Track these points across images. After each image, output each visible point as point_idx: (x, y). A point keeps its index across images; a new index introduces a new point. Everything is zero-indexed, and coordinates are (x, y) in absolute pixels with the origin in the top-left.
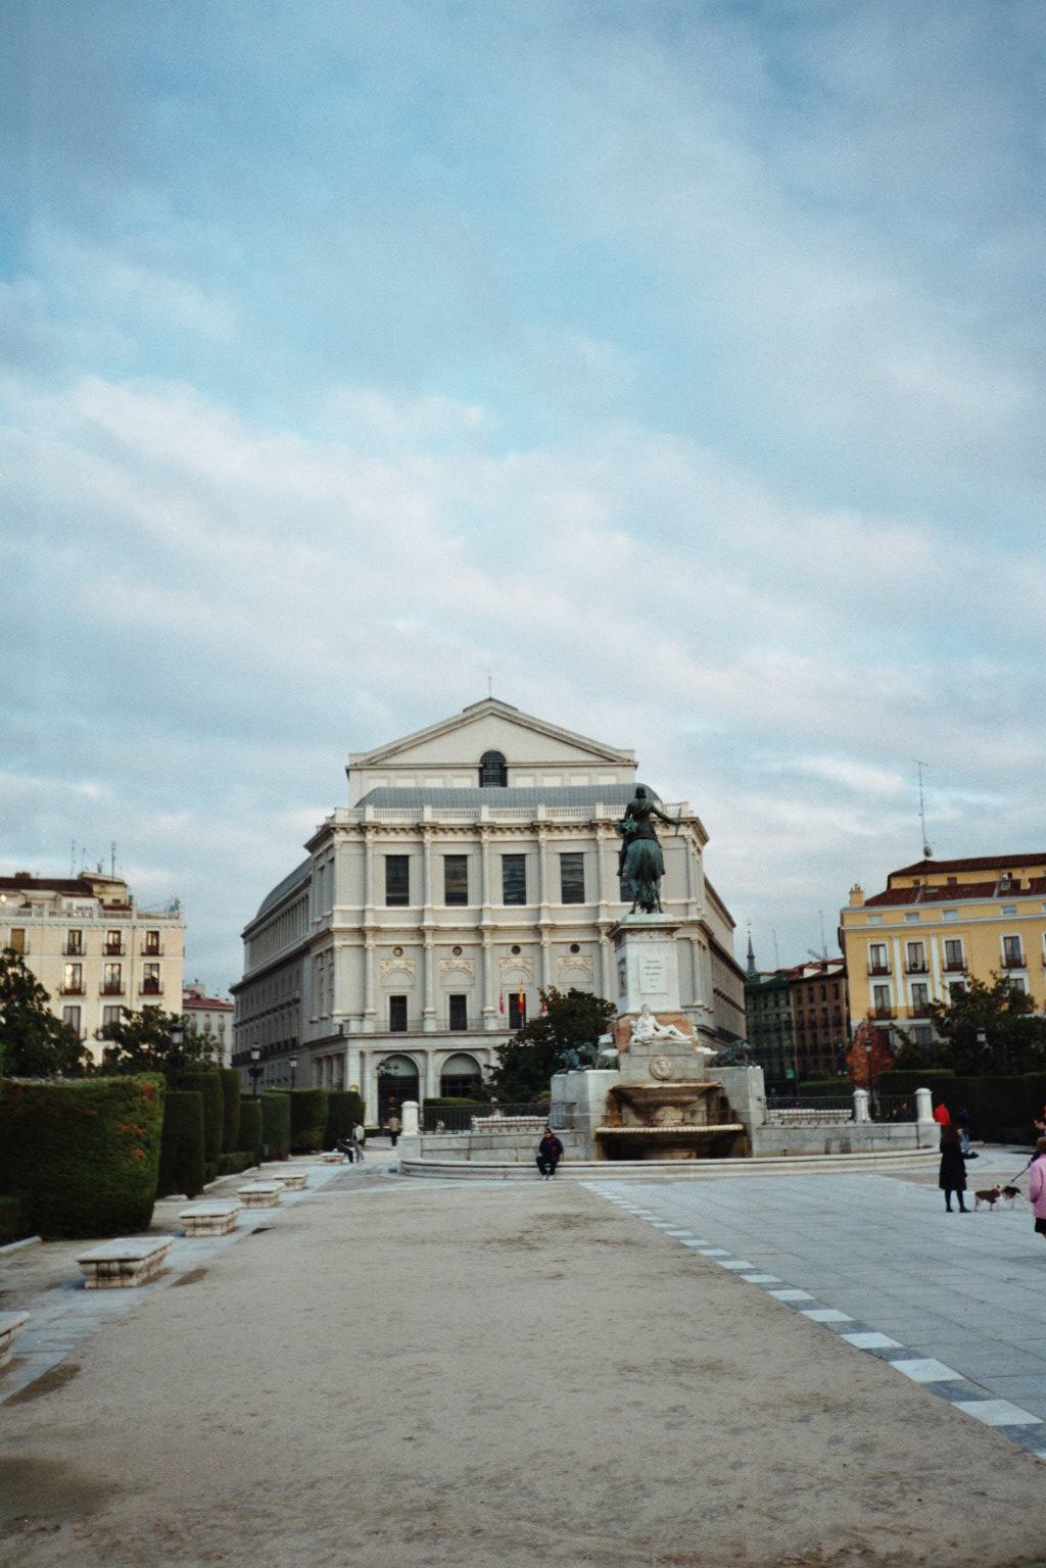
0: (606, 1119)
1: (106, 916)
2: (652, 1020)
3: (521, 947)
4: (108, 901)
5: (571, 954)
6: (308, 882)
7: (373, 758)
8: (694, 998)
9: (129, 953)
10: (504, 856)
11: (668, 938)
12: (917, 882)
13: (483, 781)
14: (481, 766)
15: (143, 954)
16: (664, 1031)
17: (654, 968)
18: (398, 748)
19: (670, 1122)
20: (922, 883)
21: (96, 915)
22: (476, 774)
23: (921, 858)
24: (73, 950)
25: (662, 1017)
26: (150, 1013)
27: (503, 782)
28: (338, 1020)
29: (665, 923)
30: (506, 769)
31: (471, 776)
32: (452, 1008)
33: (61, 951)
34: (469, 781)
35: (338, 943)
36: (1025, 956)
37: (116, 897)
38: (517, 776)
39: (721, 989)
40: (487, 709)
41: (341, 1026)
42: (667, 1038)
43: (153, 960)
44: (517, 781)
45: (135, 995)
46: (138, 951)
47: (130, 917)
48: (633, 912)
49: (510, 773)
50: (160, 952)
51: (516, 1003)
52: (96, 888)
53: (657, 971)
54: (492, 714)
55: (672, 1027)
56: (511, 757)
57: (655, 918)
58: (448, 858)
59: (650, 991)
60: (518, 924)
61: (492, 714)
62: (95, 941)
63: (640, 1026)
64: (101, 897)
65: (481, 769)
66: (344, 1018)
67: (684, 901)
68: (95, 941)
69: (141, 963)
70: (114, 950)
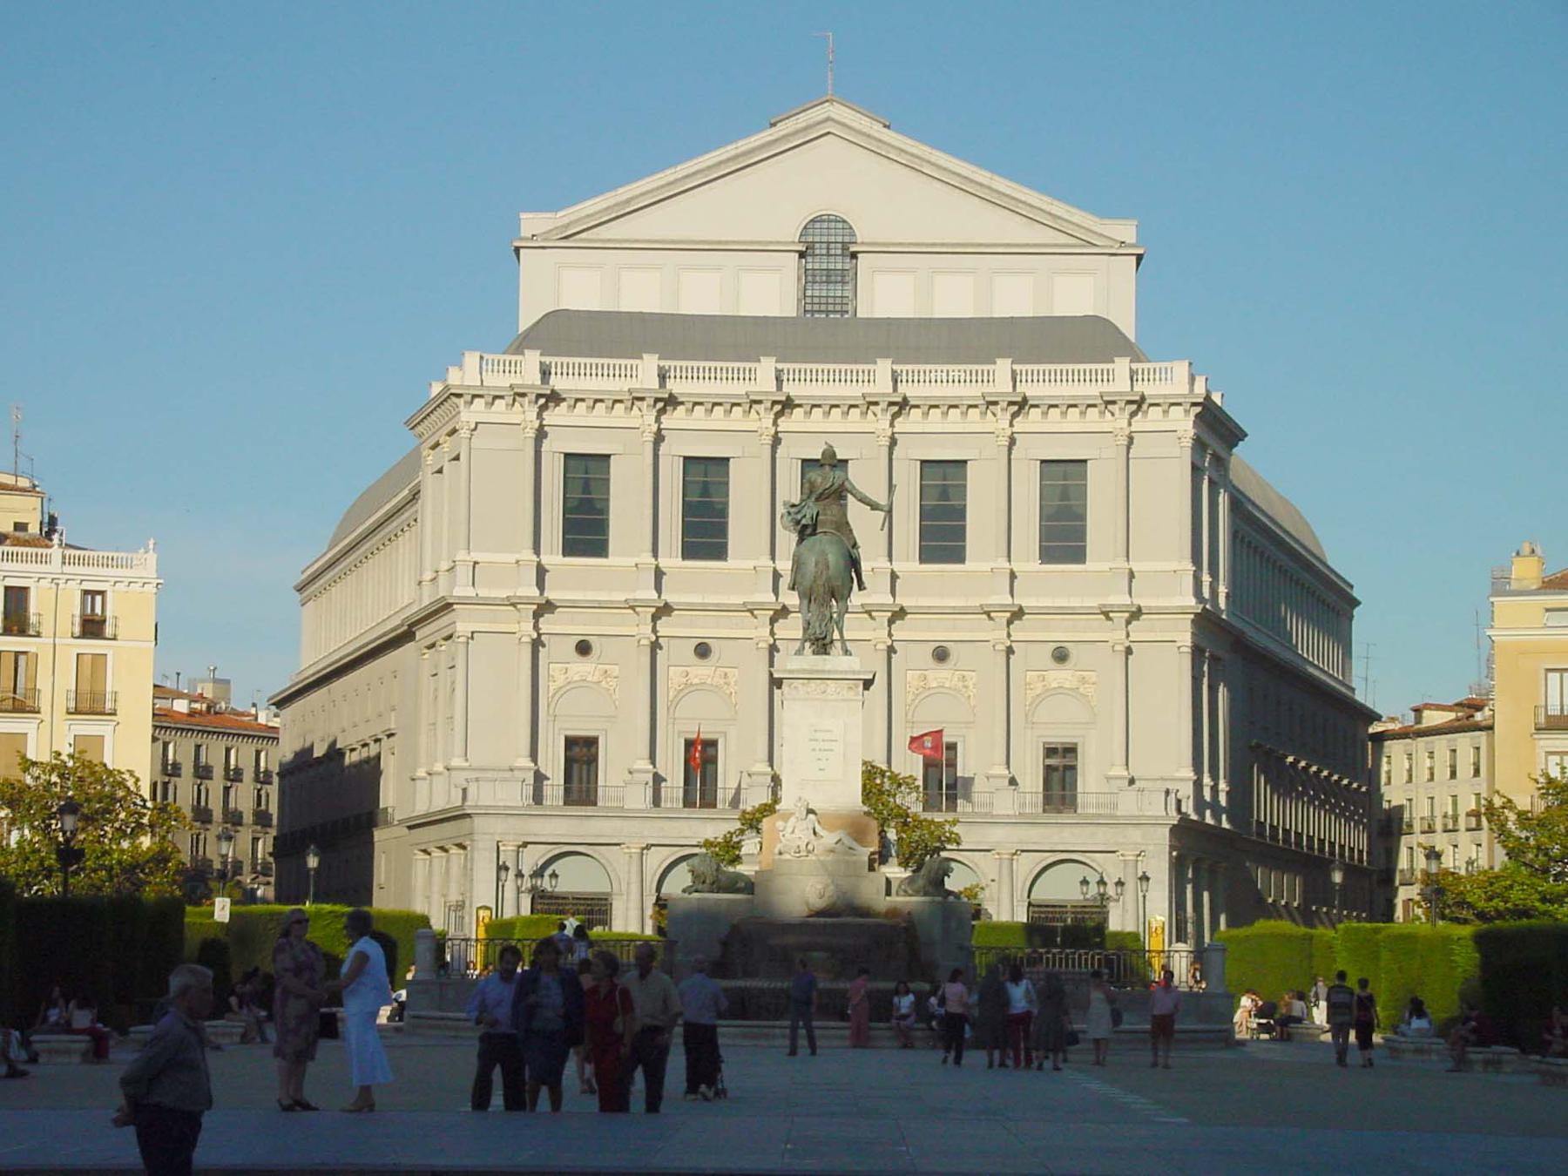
6: (415, 496)
7: (567, 226)
9: (46, 629)
11: (851, 695)
28: (460, 778)
30: (854, 255)
35: (463, 628)
41: (464, 790)
43: (92, 646)
47: (45, 560)
48: (799, 652)
50: (108, 631)
53: (827, 745)
57: (835, 661)
63: (789, 830)
65: (802, 255)
66: (473, 775)
67: (1174, 566)
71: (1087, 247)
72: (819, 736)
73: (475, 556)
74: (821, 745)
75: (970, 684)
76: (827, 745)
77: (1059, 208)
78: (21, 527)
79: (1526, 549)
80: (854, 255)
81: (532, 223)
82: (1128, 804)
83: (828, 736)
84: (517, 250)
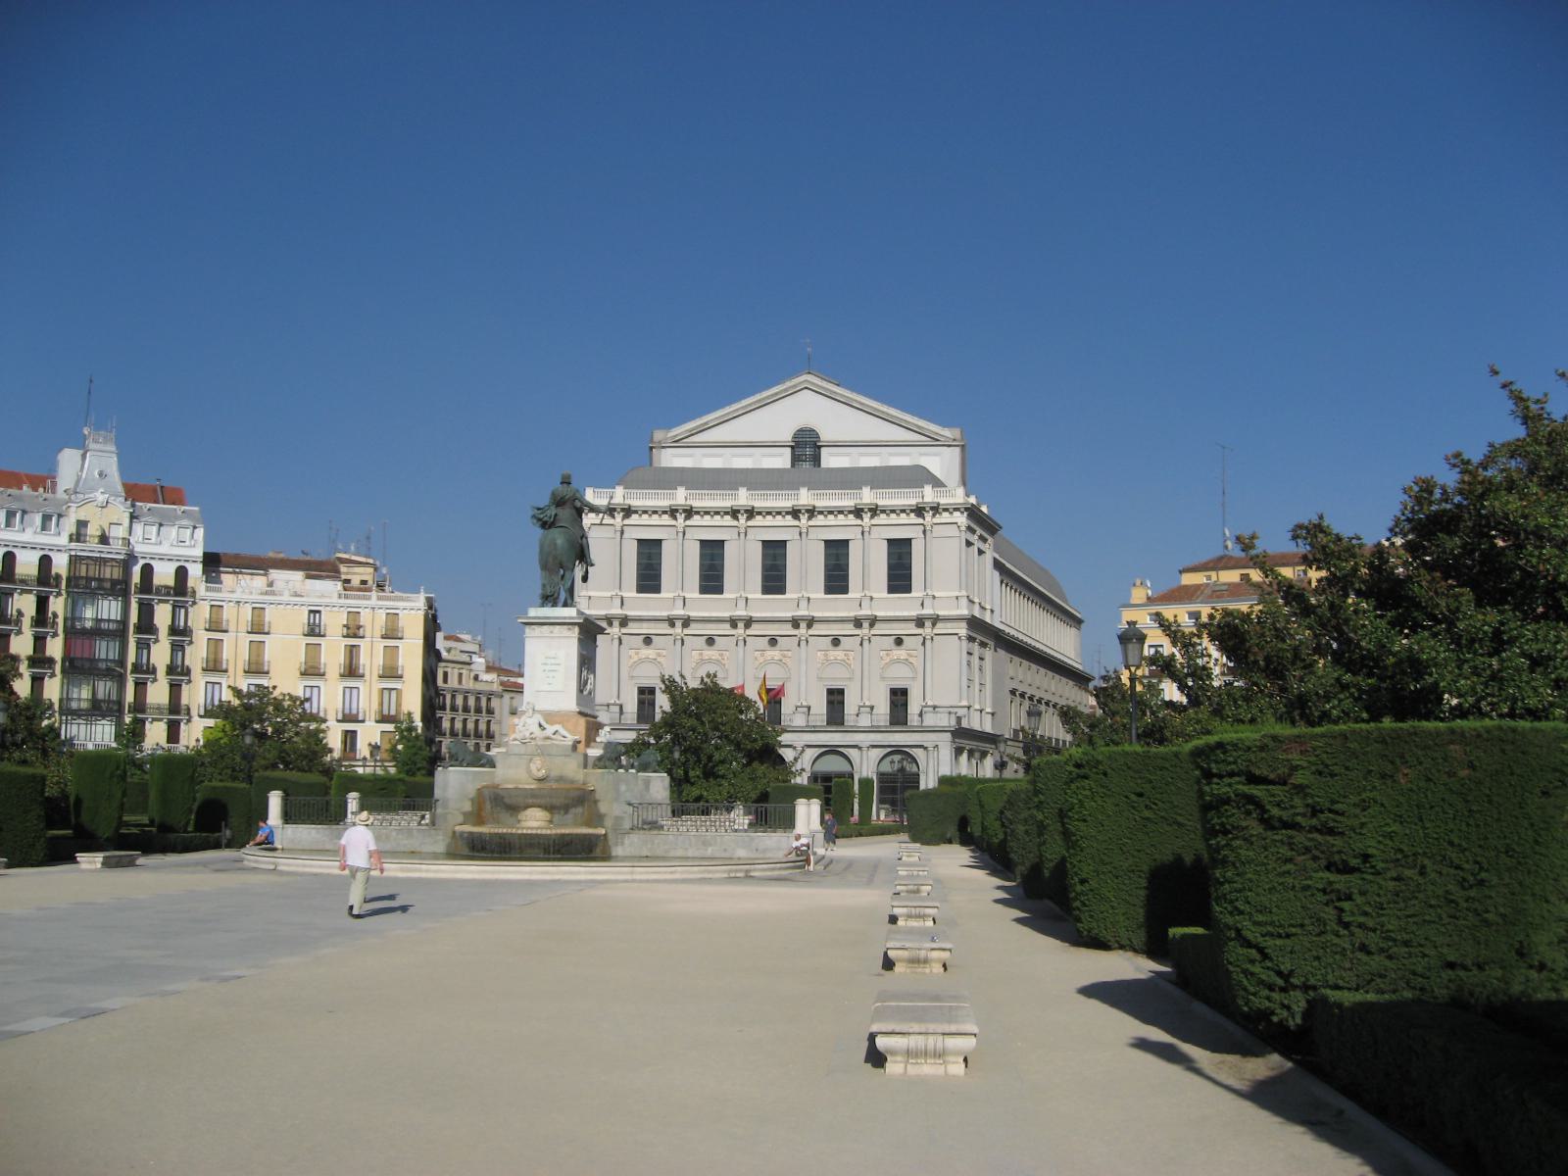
0: (468, 818)
1: (346, 597)
2: (539, 718)
3: (653, 637)
4: (356, 581)
5: (831, 647)
8: (960, 701)
9: (368, 634)
10: (702, 542)
11: (569, 633)
12: (1209, 578)
13: (796, 459)
14: (793, 444)
15: (383, 637)
16: (550, 729)
17: (552, 664)
18: (706, 423)
19: (534, 821)
20: (1214, 578)
21: (336, 595)
22: (788, 451)
23: (1220, 552)
24: (314, 631)
25: (551, 717)
26: (263, 692)
27: (816, 460)
29: (565, 618)
30: (820, 447)
31: (781, 455)
32: (830, 703)
33: (300, 631)
34: (782, 460)
36: (269, 662)
37: (364, 578)
38: (832, 455)
39: (1021, 688)
40: (801, 383)
42: (548, 738)
44: (831, 460)
45: (375, 677)
46: (378, 633)
47: (369, 598)
49: (824, 451)
51: (646, 694)
52: (343, 569)
53: (553, 667)
54: (806, 388)
55: (557, 727)
56: (825, 436)
58: (766, 544)
59: (549, 688)
60: (905, 614)
61: (806, 388)
62: (334, 622)
63: (522, 724)
64: (348, 577)
67: (957, 594)
68: (334, 622)
69: (245, 639)
70: (353, 631)
71: (935, 441)
72: (549, 661)
73: (591, 594)
74: (547, 668)
75: (851, 658)
76: (553, 667)
77: (922, 423)
78: (364, 582)
79: (1138, 582)
80: (820, 447)
81: (658, 435)
82: (930, 720)
83: (553, 661)
84: (651, 448)
